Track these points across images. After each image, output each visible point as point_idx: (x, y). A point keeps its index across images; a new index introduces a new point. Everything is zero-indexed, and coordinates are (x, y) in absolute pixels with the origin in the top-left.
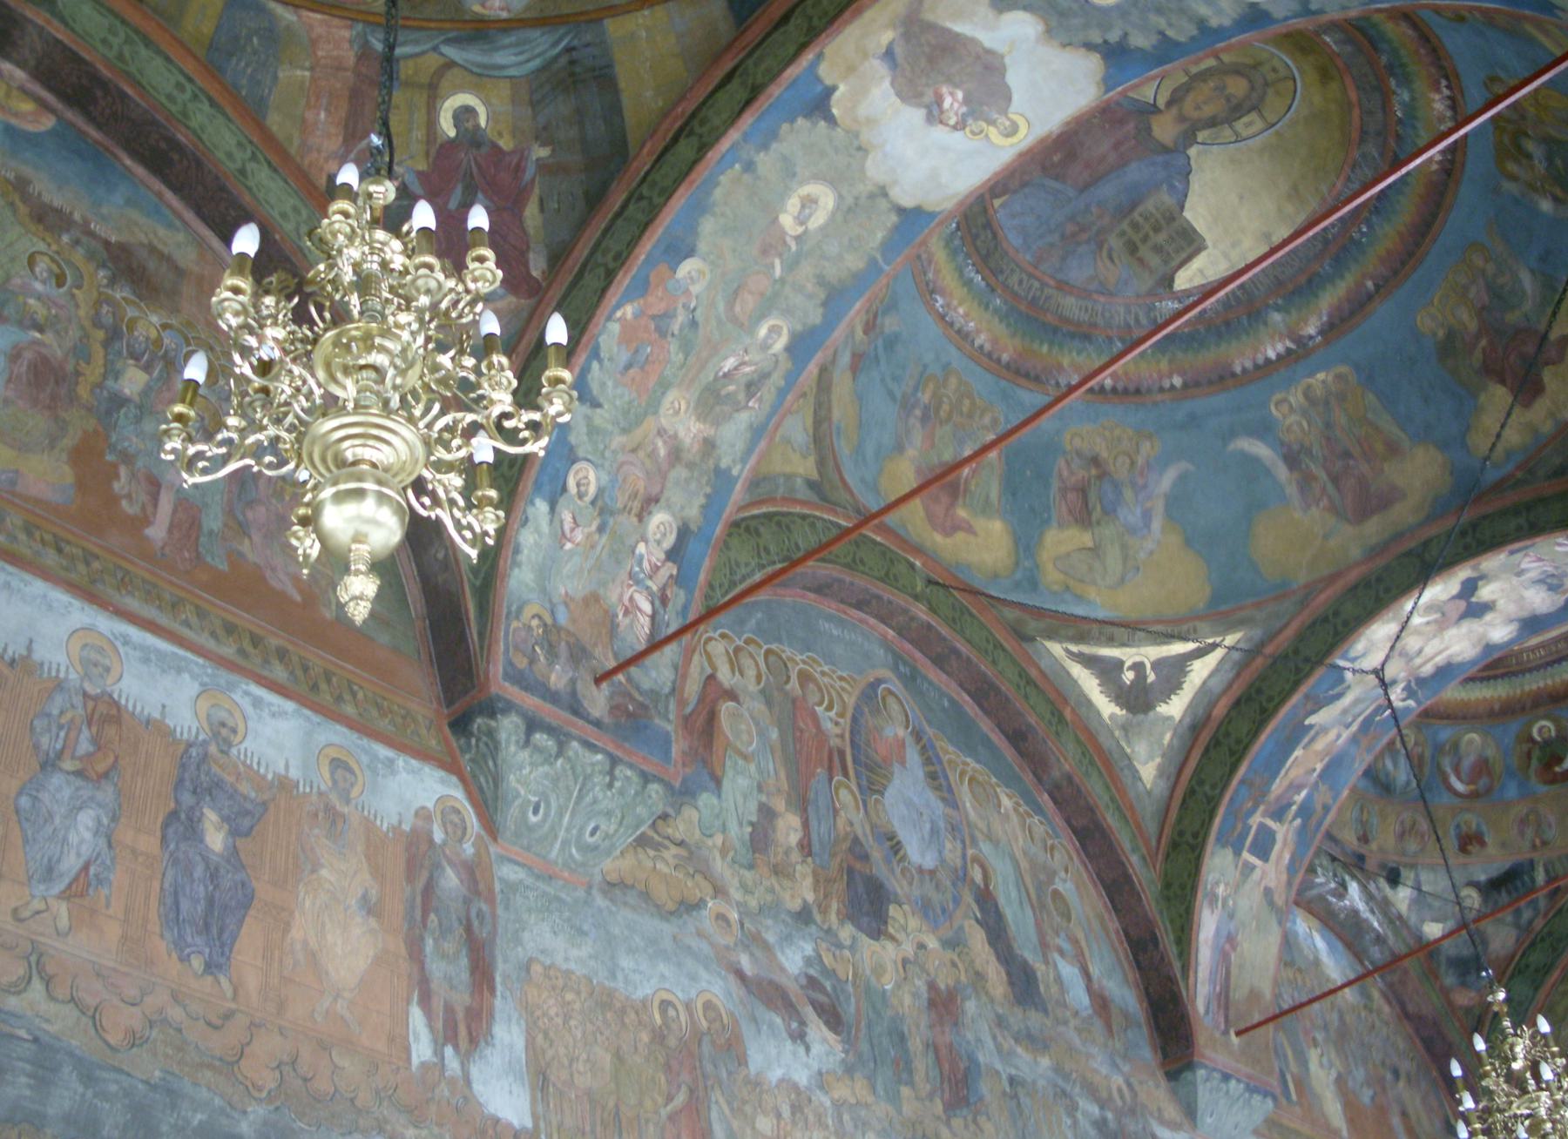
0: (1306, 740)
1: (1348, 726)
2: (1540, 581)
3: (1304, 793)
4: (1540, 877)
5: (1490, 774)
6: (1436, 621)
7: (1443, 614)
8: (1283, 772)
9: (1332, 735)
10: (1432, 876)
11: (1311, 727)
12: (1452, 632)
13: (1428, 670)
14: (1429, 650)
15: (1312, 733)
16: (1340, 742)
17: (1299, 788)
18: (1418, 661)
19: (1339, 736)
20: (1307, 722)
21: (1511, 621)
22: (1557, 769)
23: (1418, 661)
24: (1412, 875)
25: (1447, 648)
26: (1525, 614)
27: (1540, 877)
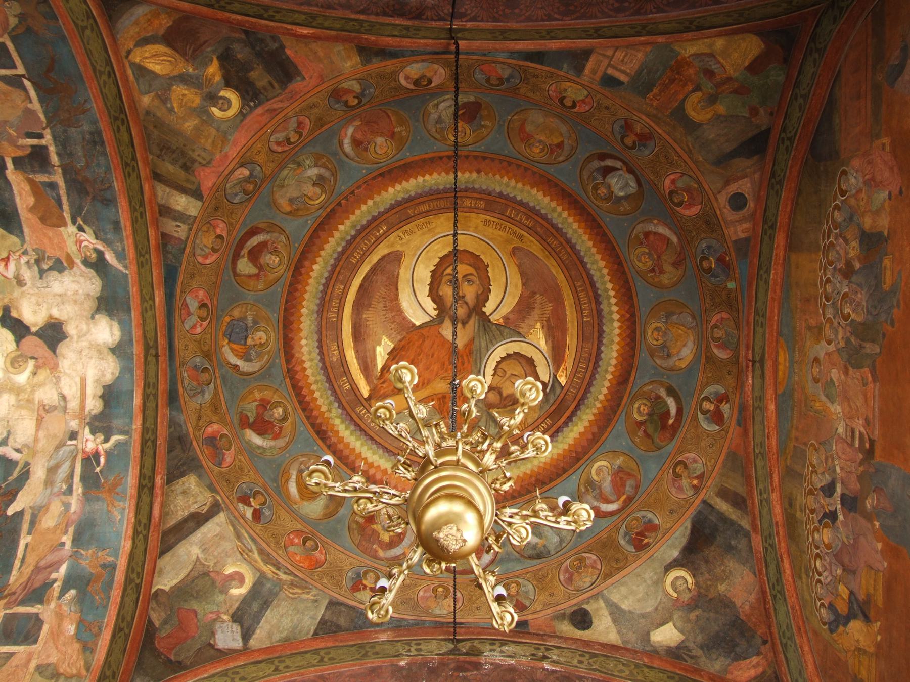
0: (25, 526)
1: (70, 491)
2: (42, 272)
3: (63, 569)
4: (723, 506)
5: (630, 475)
6: (37, 367)
7: (32, 358)
8: (17, 563)
9: (56, 507)
10: (623, 590)
11: (20, 514)
12: (65, 364)
13: (94, 405)
14: (70, 388)
15: (27, 517)
16: (73, 508)
17: (55, 566)
18: (73, 404)
19: (67, 506)
20: (10, 512)
21: (93, 318)
22: (671, 422)
23: (73, 404)
24: (602, 603)
25: (83, 382)
26: (90, 305)
27: (723, 506)
